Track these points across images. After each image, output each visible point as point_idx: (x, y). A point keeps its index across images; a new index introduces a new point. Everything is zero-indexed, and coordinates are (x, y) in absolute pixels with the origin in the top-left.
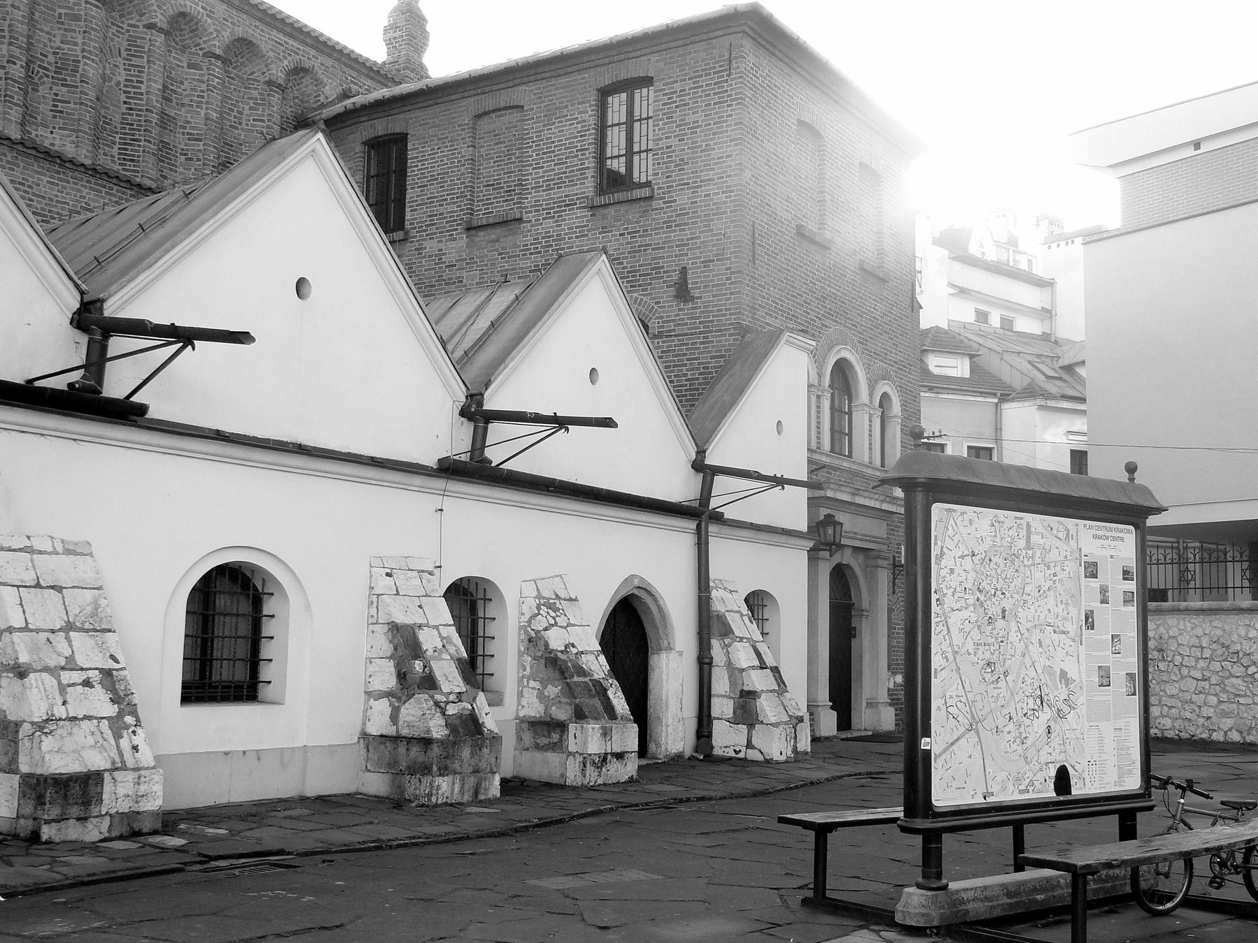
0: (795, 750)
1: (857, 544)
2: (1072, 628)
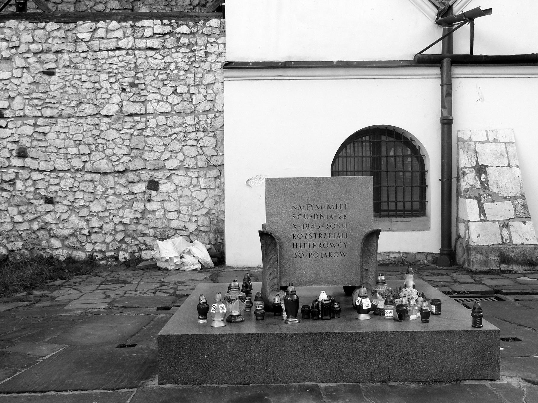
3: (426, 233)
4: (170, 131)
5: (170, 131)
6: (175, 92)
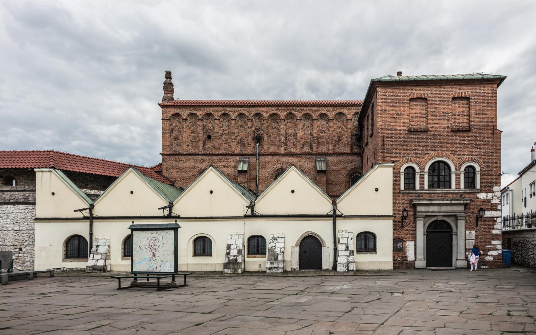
0: (348, 269)
1: (443, 214)
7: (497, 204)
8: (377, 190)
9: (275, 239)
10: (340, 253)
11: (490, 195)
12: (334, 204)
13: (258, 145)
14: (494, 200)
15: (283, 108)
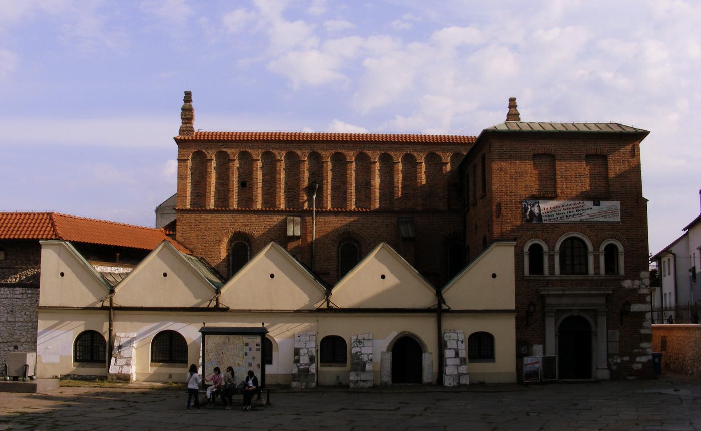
0: (459, 383)
2: (241, 356)
3: (103, 369)
4: (22, 328)
5: (22, 328)
6: (25, 314)
7: (645, 295)
8: (494, 276)
9: (360, 342)
10: (449, 362)
11: (637, 282)
12: (439, 295)
13: (315, 197)
14: (642, 289)
15: (351, 145)
